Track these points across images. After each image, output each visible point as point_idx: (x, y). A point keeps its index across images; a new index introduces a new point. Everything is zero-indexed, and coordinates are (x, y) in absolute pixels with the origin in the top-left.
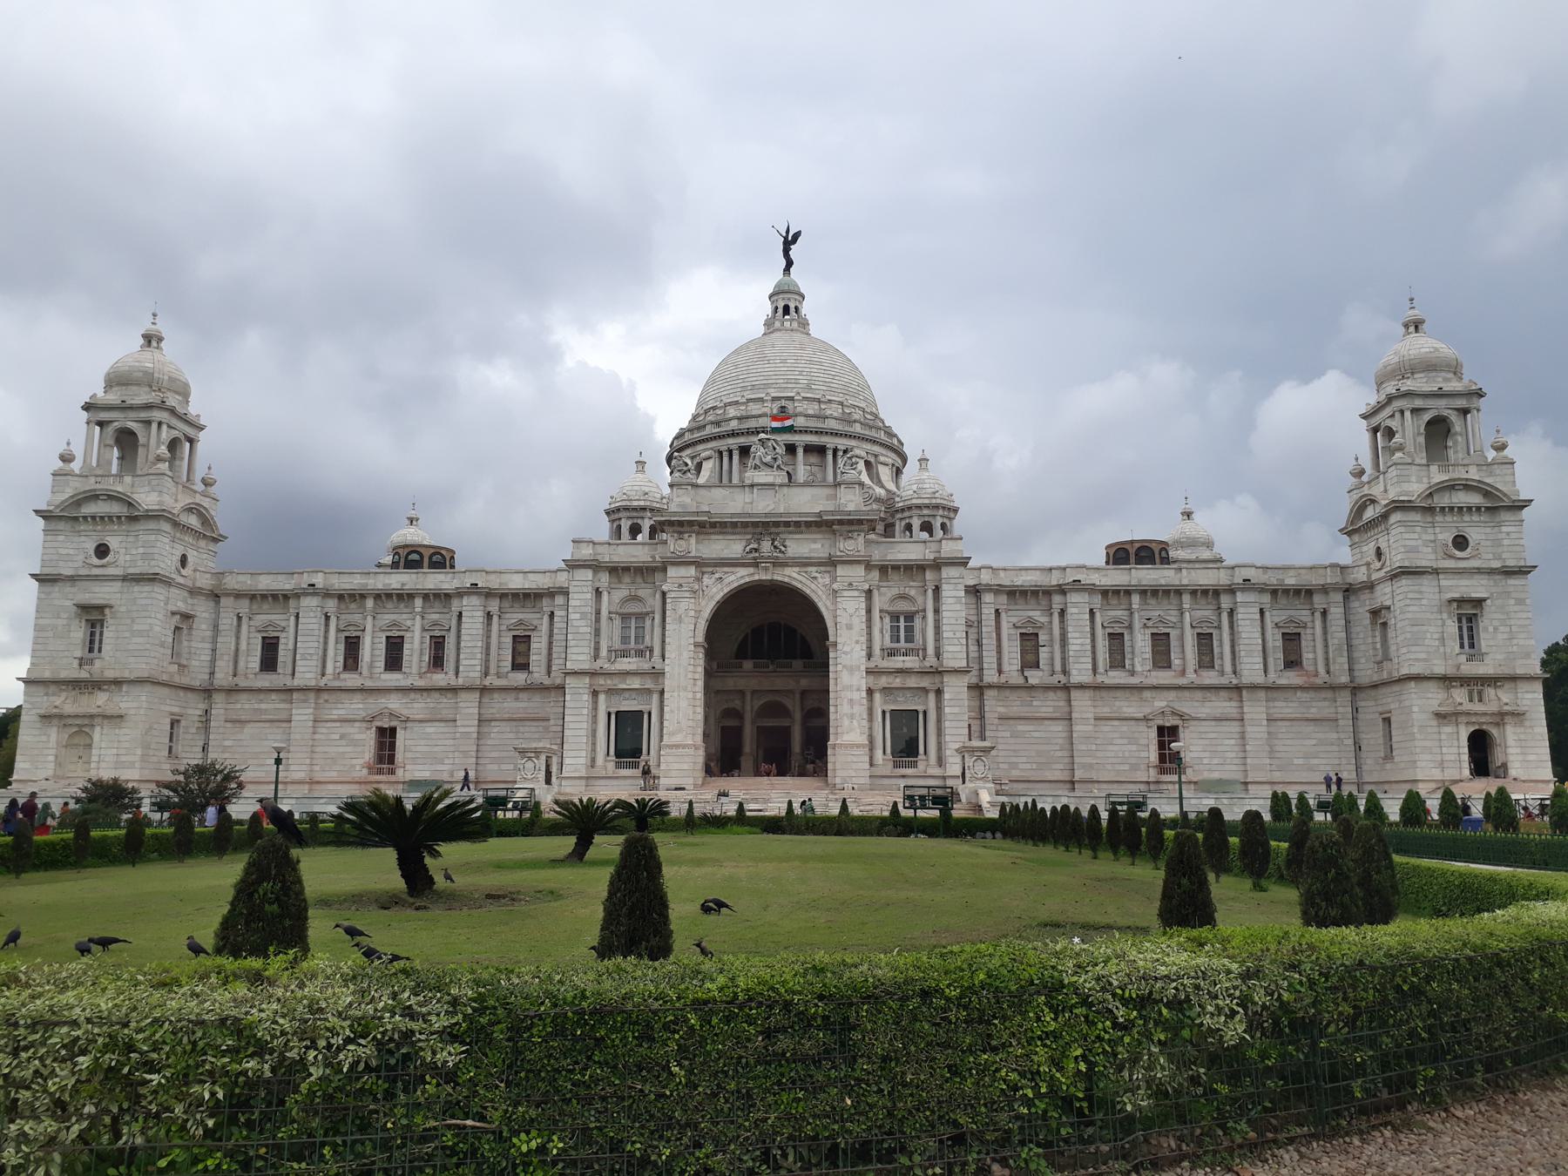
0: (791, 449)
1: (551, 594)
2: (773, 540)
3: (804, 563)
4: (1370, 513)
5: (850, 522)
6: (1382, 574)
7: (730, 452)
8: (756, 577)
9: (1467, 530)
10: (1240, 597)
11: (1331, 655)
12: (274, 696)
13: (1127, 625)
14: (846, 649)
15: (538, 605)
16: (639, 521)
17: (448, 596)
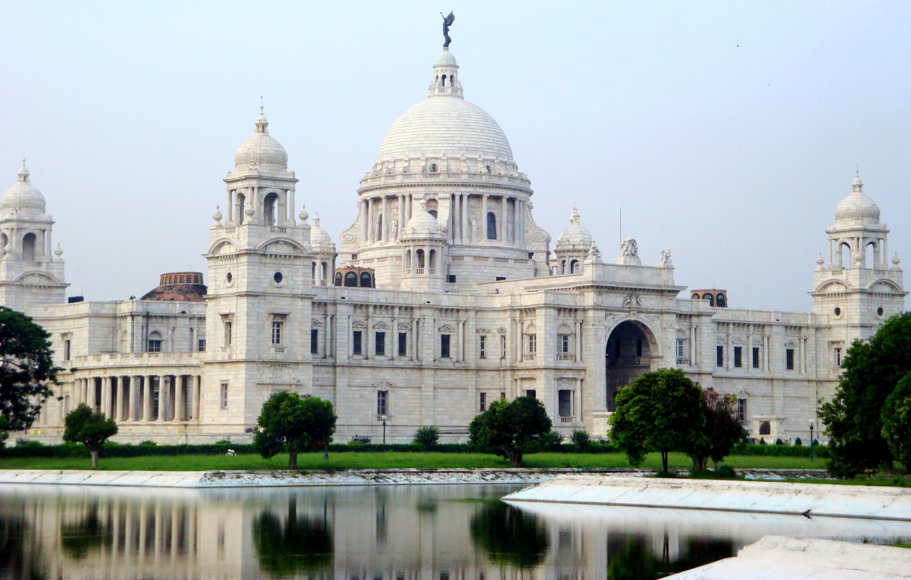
0: (497, 199)
1: (467, 310)
2: (637, 298)
3: (649, 312)
4: (834, 289)
5: (673, 291)
6: (844, 322)
7: (461, 197)
8: (628, 319)
9: (884, 305)
10: (775, 329)
11: (808, 363)
12: (323, 369)
13: (725, 342)
14: (669, 360)
15: (455, 315)
16: (434, 248)
17: (412, 308)
